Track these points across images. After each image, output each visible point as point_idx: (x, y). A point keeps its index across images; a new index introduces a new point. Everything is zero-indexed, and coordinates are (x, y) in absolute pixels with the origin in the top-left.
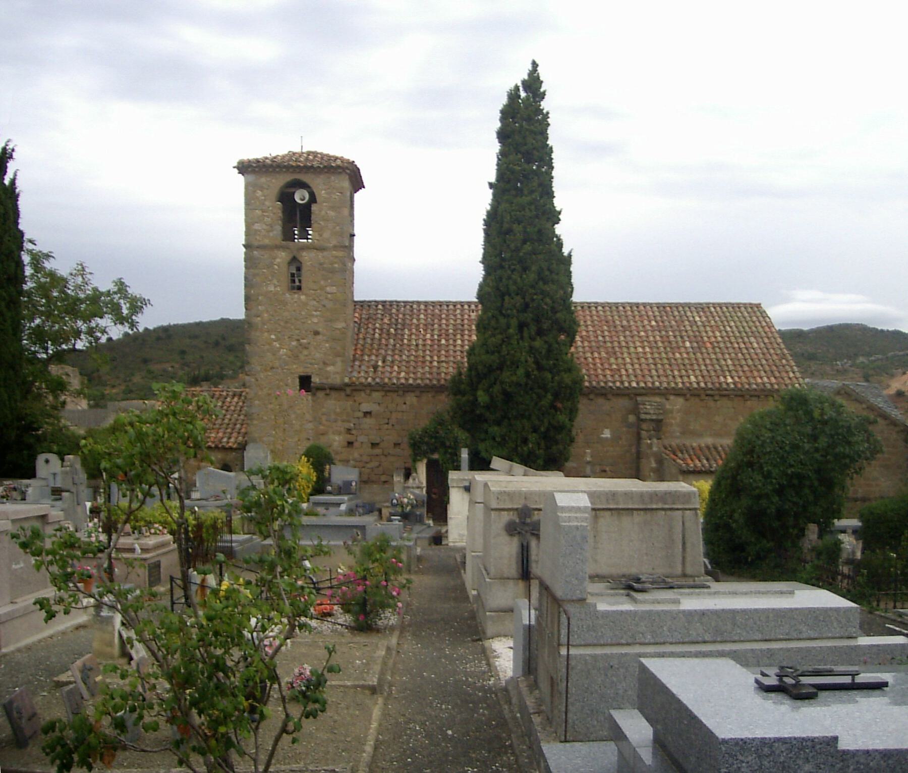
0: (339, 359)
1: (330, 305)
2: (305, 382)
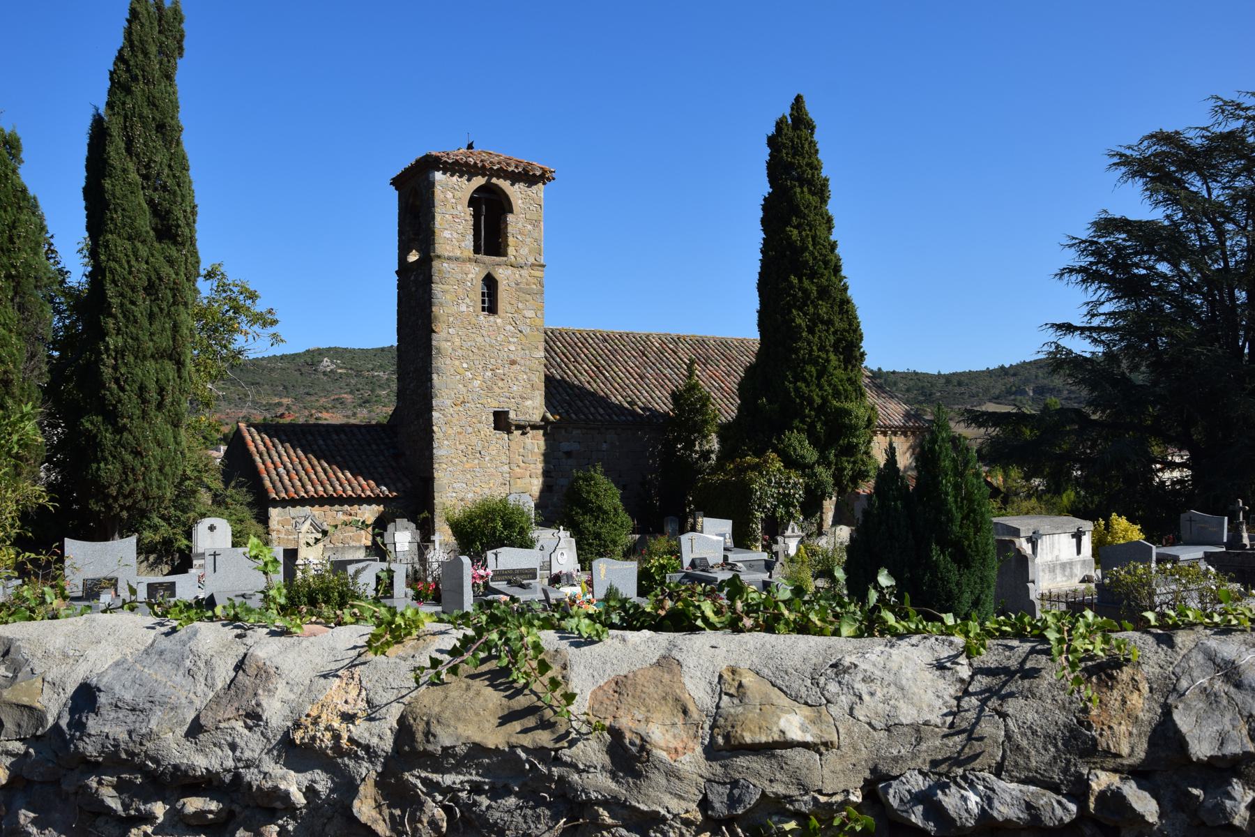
0: (537, 392)
1: (527, 330)
2: (501, 421)
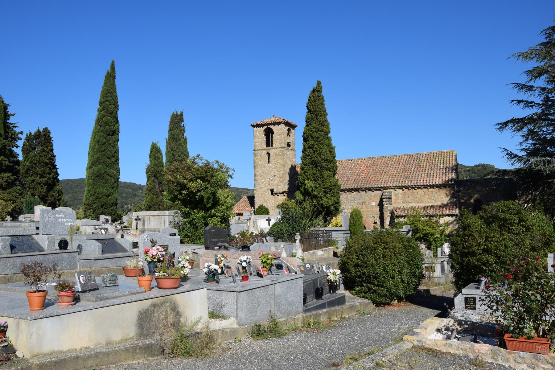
1: (279, 166)
2: (272, 191)
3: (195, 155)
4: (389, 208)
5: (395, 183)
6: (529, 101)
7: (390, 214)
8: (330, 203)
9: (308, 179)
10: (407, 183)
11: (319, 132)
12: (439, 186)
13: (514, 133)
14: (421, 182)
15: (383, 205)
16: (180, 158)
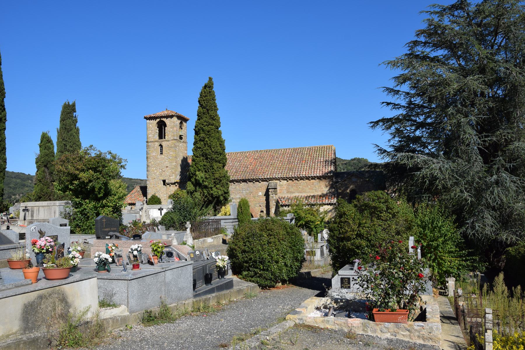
1: (171, 158)
2: (164, 181)
3: (88, 146)
4: (274, 198)
5: (280, 174)
6: (397, 103)
7: (275, 204)
8: (220, 193)
9: (199, 170)
10: (291, 175)
11: (210, 126)
12: (319, 178)
13: (384, 131)
14: (303, 174)
15: (269, 195)
16: (72, 149)
